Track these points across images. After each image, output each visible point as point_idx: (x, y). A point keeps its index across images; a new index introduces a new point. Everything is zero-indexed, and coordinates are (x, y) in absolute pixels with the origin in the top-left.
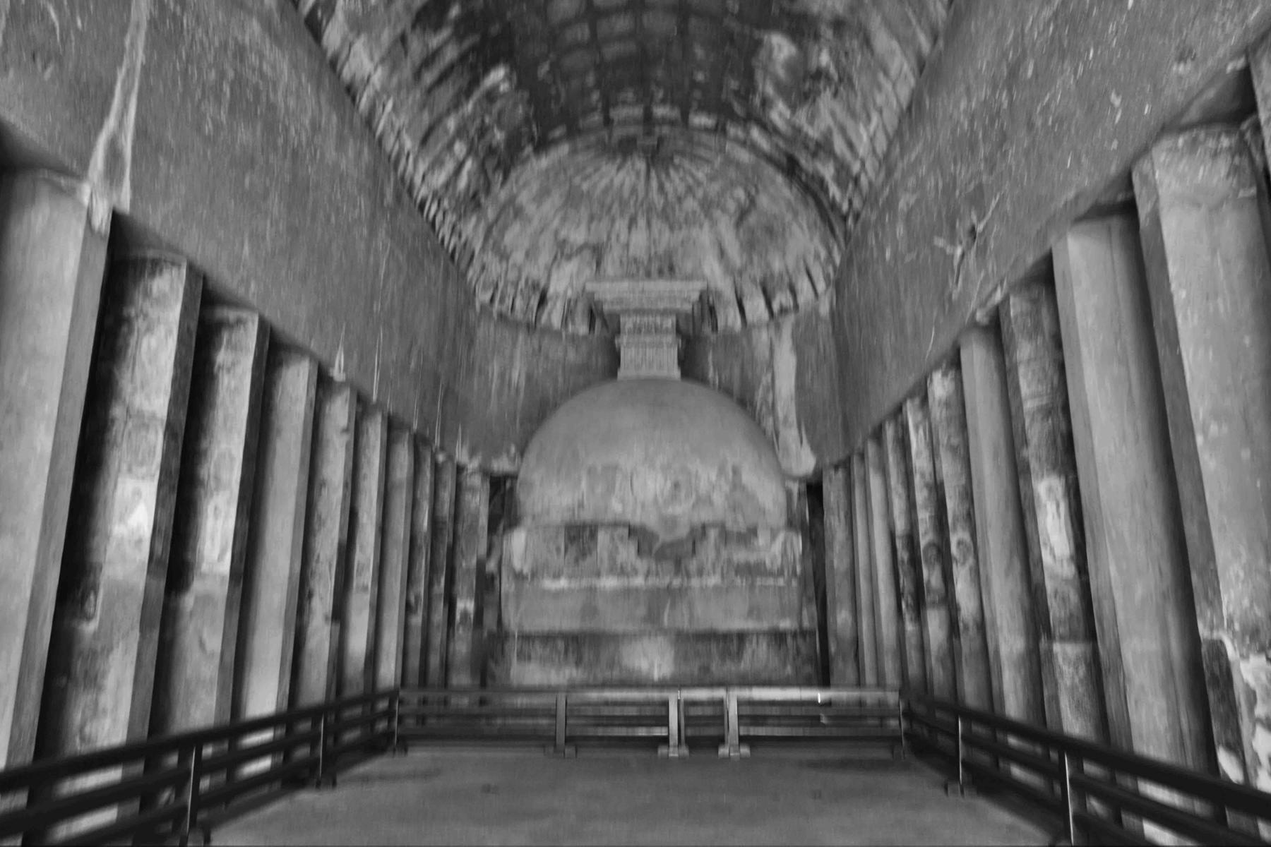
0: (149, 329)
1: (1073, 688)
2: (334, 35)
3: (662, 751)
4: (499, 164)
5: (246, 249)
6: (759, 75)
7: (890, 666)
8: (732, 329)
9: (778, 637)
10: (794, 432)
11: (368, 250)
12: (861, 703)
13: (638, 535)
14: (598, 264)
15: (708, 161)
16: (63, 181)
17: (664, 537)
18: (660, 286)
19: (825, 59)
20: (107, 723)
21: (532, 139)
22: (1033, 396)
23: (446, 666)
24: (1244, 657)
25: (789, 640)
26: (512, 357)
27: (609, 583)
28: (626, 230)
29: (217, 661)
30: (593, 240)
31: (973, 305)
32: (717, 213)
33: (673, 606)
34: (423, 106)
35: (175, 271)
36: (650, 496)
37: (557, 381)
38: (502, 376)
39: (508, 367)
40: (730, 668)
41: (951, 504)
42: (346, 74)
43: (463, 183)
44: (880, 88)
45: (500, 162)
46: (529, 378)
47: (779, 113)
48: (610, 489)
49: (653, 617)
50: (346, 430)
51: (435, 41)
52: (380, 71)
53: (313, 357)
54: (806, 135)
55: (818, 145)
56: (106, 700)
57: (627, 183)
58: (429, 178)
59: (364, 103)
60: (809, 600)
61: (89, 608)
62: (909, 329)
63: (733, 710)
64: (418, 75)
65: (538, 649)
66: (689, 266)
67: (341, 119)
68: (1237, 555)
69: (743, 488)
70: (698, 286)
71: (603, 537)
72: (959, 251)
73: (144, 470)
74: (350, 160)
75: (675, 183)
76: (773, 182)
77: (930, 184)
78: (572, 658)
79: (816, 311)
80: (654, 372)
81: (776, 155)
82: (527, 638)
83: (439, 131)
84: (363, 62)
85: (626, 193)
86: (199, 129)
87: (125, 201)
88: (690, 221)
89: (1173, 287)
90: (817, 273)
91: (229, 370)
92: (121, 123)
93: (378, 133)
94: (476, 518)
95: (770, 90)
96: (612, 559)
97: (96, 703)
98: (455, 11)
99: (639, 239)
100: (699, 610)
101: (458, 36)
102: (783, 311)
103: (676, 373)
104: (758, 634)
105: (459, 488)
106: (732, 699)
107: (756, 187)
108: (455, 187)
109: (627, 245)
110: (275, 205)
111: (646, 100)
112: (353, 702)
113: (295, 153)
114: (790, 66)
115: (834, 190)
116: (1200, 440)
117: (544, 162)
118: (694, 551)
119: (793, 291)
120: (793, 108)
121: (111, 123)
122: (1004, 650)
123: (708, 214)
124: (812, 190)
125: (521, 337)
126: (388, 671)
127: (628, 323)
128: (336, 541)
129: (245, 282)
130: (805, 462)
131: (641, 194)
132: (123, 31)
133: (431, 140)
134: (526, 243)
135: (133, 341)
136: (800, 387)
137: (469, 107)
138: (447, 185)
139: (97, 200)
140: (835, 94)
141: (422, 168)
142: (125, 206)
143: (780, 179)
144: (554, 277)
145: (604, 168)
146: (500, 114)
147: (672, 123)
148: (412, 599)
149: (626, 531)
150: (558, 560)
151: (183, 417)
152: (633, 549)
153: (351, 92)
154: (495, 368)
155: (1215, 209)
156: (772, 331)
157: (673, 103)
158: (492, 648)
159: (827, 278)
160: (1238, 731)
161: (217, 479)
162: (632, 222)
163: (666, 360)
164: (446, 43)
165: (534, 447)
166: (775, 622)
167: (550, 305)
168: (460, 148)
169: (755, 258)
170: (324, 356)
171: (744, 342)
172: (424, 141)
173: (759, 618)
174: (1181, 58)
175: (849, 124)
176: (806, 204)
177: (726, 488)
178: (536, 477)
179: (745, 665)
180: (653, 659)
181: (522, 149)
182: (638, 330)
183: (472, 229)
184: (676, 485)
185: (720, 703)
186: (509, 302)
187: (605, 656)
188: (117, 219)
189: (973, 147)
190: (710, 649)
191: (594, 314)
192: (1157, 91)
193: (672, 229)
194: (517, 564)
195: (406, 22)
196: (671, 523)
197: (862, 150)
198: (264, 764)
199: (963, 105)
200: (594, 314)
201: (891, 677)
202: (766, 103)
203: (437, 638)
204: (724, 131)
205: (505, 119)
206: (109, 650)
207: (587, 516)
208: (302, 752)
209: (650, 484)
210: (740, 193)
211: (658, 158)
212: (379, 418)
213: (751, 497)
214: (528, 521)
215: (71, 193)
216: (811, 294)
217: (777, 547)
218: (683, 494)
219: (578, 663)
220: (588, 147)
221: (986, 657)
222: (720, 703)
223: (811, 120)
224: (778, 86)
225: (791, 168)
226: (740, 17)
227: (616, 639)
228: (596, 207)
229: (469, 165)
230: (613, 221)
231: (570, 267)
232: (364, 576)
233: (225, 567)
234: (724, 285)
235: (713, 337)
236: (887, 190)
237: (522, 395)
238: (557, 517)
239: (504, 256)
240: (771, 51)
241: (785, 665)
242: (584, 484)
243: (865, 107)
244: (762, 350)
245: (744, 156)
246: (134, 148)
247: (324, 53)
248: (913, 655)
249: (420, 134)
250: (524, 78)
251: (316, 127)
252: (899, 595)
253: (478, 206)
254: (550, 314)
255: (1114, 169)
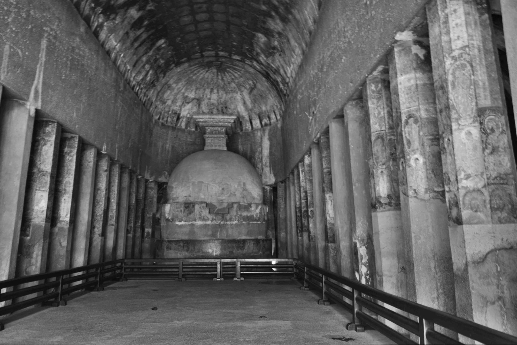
0: (45, 144)
1: (333, 256)
2: (103, 36)
3: (215, 279)
4: (162, 71)
5: (75, 115)
6: (255, 45)
7: (295, 251)
8: (248, 130)
9: (257, 242)
10: (268, 169)
11: (114, 107)
12: (287, 263)
13: (209, 206)
14: (199, 105)
15: (239, 71)
16: (21, 102)
17: (219, 207)
18: (221, 117)
19: (276, 43)
20: (34, 268)
21: (174, 63)
22: (326, 168)
23: (141, 252)
24: (361, 247)
25: (261, 243)
26: (166, 140)
27: (199, 223)
28: (209, 93)
29: (65, 249)
30: (197, 97)
31: (313, 136)
32: (243, 89)
33: (221, 231)
34: (134, 54)
35: (53, 125)
36: (214, 192)
37: (183, 148)
38: (163, 147)
39: (165, 143)
40: (240, 251)
41: (309, 198)
42: (107, 47)
43: (148, 79)
44: (293, 57)
45: (162, 70)
46: (173, 147)
47: (262, 58)
48: (200, 190)
49: (214, 235)
50: (106, 171)
51: (138, 33)
52: (119, 45)
53: (96, 147)
54: (272, 67)
55: (275, 70)
56: (33, 261)
57: (210, 77)
58: (135, 78)
59: (113, 55)
60: (272, 228)
61: (28, 233)
62: (300, 140)
63: (239, 265)
64: (132, 44)
65: (174, 246)
66: (232, 107)
67: (105, 64)
68: (360, 219)
69: (247, 190)
70: (235, 117)
71: (197, 207)
72: (311, 118)
73: (44, 189)
74: (109, 77)
75: (228, 77)
76: (262, 80)
77: (305, 94)
78: (185, 248)
79: (276, 126)
80: (217, 148)
81: (263, 72)
82: (170, 242)
83: (140, 62)
84: (114, 43)
85: (209, 81)
86: (61, 77)
87: (39, 106)
88: (233, 91)
89: (350, 144)
90: (277, 112)
91: (69, 154)
92: (38, 82)
93: (118, 64)
94: (152, 198)
95: (259, 51)
96: (200, 215)
97: (30, 261)
98: (146, 23)
99: (214, 97)
100: (230, 232)
101: (147, 31)
102: (266, 125)
103: (225, 148)
104: (250, 240)
105: (146, 188)
106: (238, 263)
107: (256, 81)
108: (146, 79)
109: (210, 99)
110: (84, 98)
111: (216, 49)
112: (108, 263)
113: (90, 79)
114: (264, 43)
115: (281, 86)
116: (354, 187)
117: (179, 70)
118: (229, 213)
119: (269, 118)
120: (267, 57)
121: (35, 82)
122: (319, 246)
123: (240, 90)
124: (274, 84)
125: (170, 132)
126: (120, 253)
127: (208, 130)
128: (103, 210)
129: (74, 125)
130: (270, 179)
131: (215, 80)
132: (39, 53)
133: (137, 66)
134: (172, 97)
135: (40, 147)
136: (271, 153)
137: (151, 53)
138: (142, 80)
139: (31, 106)
140: (280, 55)
141: (134, 75)
142: (40, 108)
143: (264, 79)
144: (183, 109)
145: (202, 72)
146: (162, 54)
147: (225, 57)
148: (129, 229)
149: (204, 205)
150: (181, 215)
151: (55, 171)
152: (207, 211)
153: (108, 53)
154: (160, 144)
155: (360, 123)
156: (262, 131)
157: (226, 52)
158: (158, 244)
159: (280, 115)
160: (358, 267)
161: (65, 190)
162: (212, 91)
163: (221, 144)
164: (142, 33)
165: (173, 175)
166: (256, 237)
167: (181, 120)
168: (147, 67)
169: (256, 105)
170: (99, 146)
171: (252, 135)
172: (134, 66)
173: (251, 236)
174: (351, 82)
175: (284, 65)
176: (273, 88)
177: (241, 190)
178: (174, 185)
179: (245, 251)
180: (213, 249)
181: (171, 65)
182: (212, 133)
183: (152, 93)
184: (223, 189)
185: (234, 263)
186: (165, 119)
187: (197, 248)
188: (37, 111)
189: (314, 86)
190: (234, 246)
191: (197, 126)
192: (347, 89)
193: (226, 93)
194: (167, 216)
195: (129, 27)
196: (221, 202)
197: (289, 75)
198: (80, 282)
199: (312, 72)
200: (197, 126)
201: (296, 257)
202: (258, 54)
203: (138, 242)
204: (244, 62)
205: (164, 56)
206: (34, 246)
207: (191, 199)
208: (92, 279)
209: (214, 188)
210: (251, 82)
211: (221, 69)
212: (118, 165)
213: (249, 193)
214: (171, 201)
215: (23, 105)
216: (275, 120)
217: (258, 211)
218: (225, 193)
219: (187, 251)
220: (196, 64)
221: (315, 248)
222: (234, 263)
223: (273, 61)
224: (261, 49)
225: (267, 76)
226: (247, 27)
227: (200, 242)
228: (198, 86)
229: (151, 72)
230: (205, 90)
231: (189, 106)
232: (112, 221)
233: (68, 219)
234: (245, 114)
235: (241, 133)
236: (295, 91)
237: (170, 153)
238: (181, 200)
239: (164, 103)
240: (258, 38)
241: (259, 251)
242: (191, 189)
243: (289, 61)
244: (258, 138)
245: (251, 70)
246: (42, 88)
247: (99, 41)
248: (300, 247)
249: (133, 64)
250: (171, 42)
251: (97, 69)
252: (297, 227)
253: (154, 86)
254: (181, 124)
255: (340, 107)
